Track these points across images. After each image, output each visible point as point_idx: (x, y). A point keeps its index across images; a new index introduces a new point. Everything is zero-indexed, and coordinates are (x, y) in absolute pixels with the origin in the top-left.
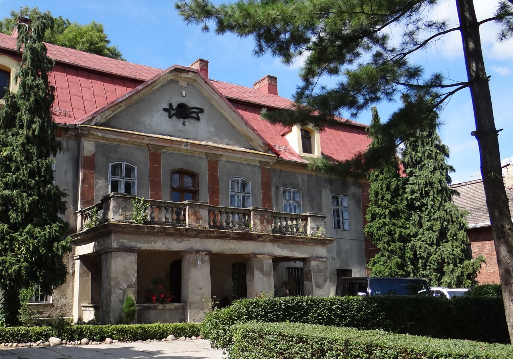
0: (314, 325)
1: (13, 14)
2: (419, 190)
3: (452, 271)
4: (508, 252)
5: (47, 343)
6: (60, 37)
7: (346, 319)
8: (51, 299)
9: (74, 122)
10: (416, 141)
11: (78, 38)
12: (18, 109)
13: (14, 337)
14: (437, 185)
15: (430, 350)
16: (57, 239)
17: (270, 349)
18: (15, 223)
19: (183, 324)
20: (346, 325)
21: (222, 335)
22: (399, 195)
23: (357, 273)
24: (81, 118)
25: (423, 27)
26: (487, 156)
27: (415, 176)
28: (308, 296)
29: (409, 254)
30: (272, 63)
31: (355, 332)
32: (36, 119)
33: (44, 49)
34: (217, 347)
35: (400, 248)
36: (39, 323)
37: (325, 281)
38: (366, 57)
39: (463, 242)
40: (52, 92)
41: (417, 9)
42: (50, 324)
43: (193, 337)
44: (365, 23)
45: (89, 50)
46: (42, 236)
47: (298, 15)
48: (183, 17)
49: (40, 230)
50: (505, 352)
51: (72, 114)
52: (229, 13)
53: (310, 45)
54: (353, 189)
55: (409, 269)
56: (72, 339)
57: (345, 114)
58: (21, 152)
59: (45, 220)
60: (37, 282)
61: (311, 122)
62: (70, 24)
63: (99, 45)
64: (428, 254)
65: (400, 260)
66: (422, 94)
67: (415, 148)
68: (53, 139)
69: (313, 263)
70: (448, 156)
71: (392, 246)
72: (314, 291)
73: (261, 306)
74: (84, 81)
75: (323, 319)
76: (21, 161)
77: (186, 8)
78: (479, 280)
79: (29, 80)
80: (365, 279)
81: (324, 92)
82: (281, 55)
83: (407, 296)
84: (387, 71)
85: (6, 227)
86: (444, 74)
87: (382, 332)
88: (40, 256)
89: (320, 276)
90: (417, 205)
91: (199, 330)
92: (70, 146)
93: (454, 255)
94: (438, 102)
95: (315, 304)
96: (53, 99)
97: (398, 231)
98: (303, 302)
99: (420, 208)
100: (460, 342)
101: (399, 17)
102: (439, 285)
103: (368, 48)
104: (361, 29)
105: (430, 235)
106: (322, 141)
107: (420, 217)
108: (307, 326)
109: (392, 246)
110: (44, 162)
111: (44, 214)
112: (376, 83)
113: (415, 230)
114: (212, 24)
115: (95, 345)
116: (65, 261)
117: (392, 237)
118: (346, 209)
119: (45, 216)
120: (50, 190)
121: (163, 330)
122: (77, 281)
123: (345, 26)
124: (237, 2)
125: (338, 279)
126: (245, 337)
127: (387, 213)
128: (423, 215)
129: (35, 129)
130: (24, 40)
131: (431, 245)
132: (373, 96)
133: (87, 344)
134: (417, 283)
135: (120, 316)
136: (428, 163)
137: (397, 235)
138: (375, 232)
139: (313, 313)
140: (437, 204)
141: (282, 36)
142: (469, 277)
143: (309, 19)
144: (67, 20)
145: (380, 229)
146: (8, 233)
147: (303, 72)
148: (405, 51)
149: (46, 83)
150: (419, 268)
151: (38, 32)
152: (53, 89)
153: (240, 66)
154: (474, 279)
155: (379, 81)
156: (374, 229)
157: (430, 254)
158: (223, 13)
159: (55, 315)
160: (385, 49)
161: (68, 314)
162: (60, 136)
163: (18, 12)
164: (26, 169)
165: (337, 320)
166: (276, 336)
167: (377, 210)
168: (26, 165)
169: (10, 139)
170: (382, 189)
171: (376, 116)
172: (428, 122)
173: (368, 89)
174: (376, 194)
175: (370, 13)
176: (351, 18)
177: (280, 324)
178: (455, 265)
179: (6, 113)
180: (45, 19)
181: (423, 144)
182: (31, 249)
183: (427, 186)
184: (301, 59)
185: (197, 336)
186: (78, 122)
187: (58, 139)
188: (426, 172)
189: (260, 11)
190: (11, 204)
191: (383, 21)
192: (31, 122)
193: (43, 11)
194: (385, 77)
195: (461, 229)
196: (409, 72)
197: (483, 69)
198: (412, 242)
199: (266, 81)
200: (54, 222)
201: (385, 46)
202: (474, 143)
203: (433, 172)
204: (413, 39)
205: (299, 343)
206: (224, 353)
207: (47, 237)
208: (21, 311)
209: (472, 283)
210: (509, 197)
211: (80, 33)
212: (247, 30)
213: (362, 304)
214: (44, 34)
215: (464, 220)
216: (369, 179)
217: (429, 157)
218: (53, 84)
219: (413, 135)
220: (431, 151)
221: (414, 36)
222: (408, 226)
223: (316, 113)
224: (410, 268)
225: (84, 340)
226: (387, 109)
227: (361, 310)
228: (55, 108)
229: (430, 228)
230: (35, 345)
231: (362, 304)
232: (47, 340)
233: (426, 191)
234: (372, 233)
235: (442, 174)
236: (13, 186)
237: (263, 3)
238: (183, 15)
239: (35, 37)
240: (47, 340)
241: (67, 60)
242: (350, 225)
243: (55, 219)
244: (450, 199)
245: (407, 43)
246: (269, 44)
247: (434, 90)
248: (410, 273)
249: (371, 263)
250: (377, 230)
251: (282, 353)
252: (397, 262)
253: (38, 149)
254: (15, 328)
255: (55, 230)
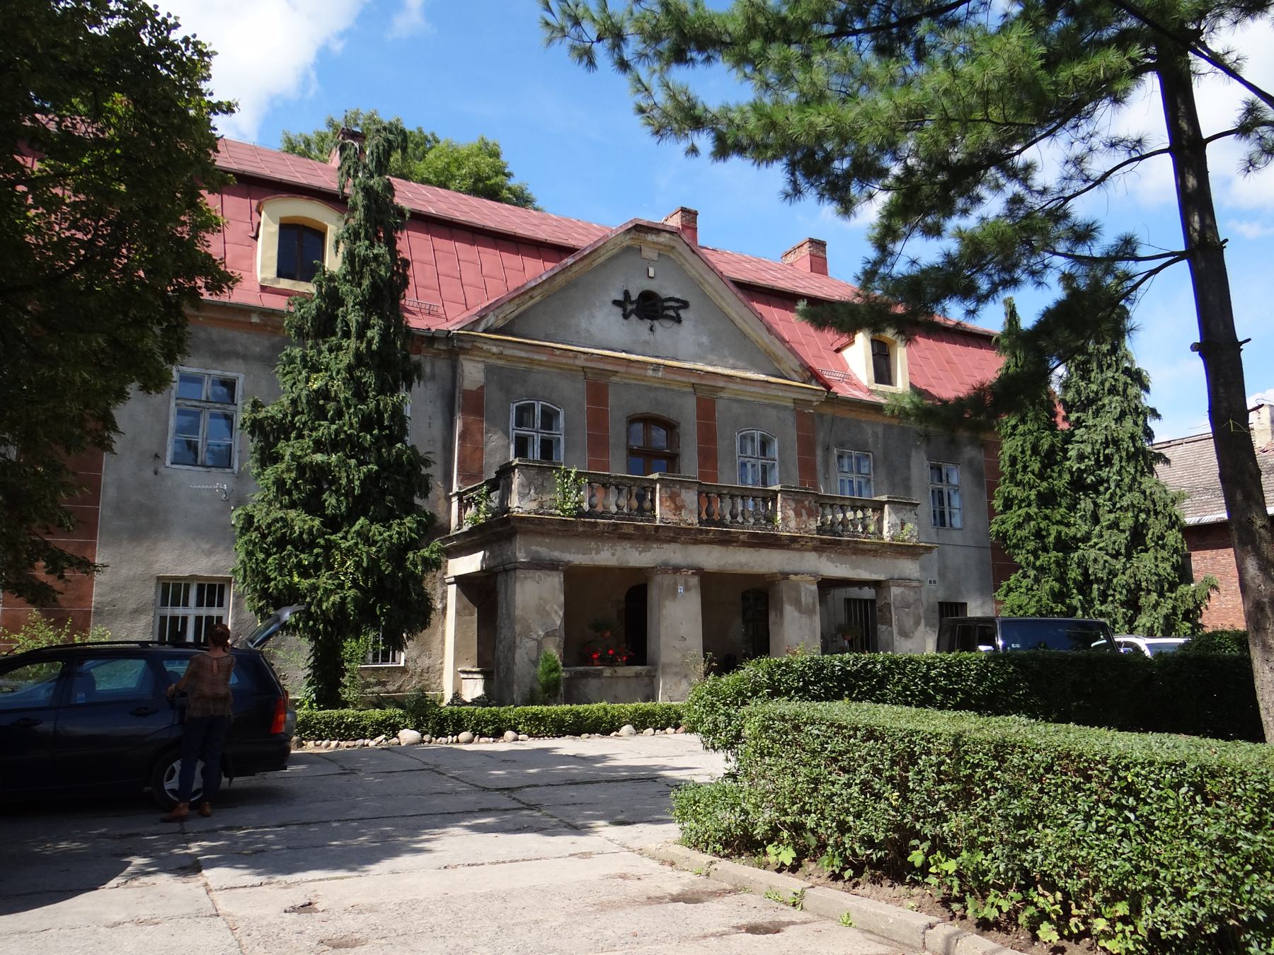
0: (895, 707)
1: (331, 123)
2: (1093, 453)
3: (1156, 606)
4: (1260, 569)
5: (395, 740)
6: (420, 167)
7: (955, 696)
8: (402, 658)
9: (445, 326)
10: (1088, 362)
11: (453, 169)
12: (341, 303)
13: (333, 729)
14: (1127, 444)
15: (1114, 754)
16: (413, 545)
17: (814, 752)
18: (335, 516)
19: (649, 705)
20: (957, 707)
21: (722, 725)
22: (1056, 463)
23: (976, 609)
24: (458, 319)
25: (1101, 147)
26: (1221, 390)
27: (1086, 427)
28: (885, 652)
29: (1074, 573)
30: (817, 215)
31: (973, 719)
32: (374, 320)
33: (390, 188)
34: (713, 747)
35: (1057, 563)
36: (379, 704)
37: (917, 624)
38: (993, 204)
39: (1176, 551)
40: (405, 270)
41: (1089, 115)
42: (401, 706)
43: (669, 730)
44: (992, 140)
45: (475, 191)
46: (384, 540)
47: (866, 125)
48: (649, 129)
49: (382, 529)
50: (1254, 758)
51: (441, 311)
52: (737, 121)
53: (889, 181)
54: (969, 452)
55: (1075, 602)
56: (441, 733)
57: (954, 311)
58: (346, 382)
59: (392, 509)
60: (375, 625)
61: (890, 326)
62: (438, 142)
63: (493, 181)
64: (1110, 573)
65: (1057, 585)
66: (1099, 273)
67: (1086, 376)
68: (406, 357)
69: (895, 591)
70: (1147, 389)
71: (1043, 559)
72: (896, 643)
73: (796, 670)
74: (464, 250)
75: (913, 695)
76: (346, 399)
77: (656, 113)
78: (1206, 623)
79: (362, 248)
80: (991, 620)
81: (914, 270)
82: (834, 199)
83: (1071, 652)
84: (1034, 231)
85: (317, 522)
86: (1141, 235)
87: (1024, 719)
88: (382, 577)
89: (908, 614)
90: (1089, 481)
91: (680, 717)
92: (437, 371)
93: (1159, 575)
94: (1128, 289)
95: (898, 667)
96: (405, 283)
97: (1054, 530)
98: (874, 664)
99: (1094, 487)
100: (1170, 739)
101: (1055, 129)
102: (1131, 632)
103: (998, 187)
104: (984, 151)
105: (1113, 538)
106: (912, 362)
107: (1095, 504)
108: (884, 708)
109: (1043, 559)
110: (389, 401)
111: (389, 498)
112: (1013, 253)
113: (1085, 528)
114: (705, 141)
115: (486, 745)
116: (428, 587)
117: (1043, 542)
118: (957, 489)
119: (390, 501)
120: (400, 454)
121: (613, 716)
122: (451, 624)
123: (954, 146)
124: (751, 100)
125: (941, 621)
126: (766, 729)
127: (1033, 497)
128: (1100, 501)
129: (373, 338)
130: (352, 171)
131: (1116, 556)
132: (1007, 277)
133: (470, 741)
134: (1090, 629)
135: (532, 690)
136: (1111, 402)
137: (1051, 539)
138: (1011, 532)
139: (894, 685)
140: (1127, 480)
141: (836, 164)
142: (1187, 616)
143: (887, 133)
144: (433, 135)
145: (1019, 526)
146: (322, 535)
147: (875, 233)
148: (1067, 193)
149: (393, 252)
150: (1092, 600)
151: (378, 158)
152: (406, 263)
153: (758, 221)
154: (1196, 620)
155: (1019, 249)
156: (1009, 527)
157: (1113, 573)
158: (725, 121)
159: (410, 687)
160: (1029, 188)
161: (433, 686)
162: (419, 352)
163: (340, 120)
164: (355, 414)
165: (938, 698)
166: (824, 728)
167: (1015, 491)
168: (356, 406)
169: (326, 357)
170: (1023, 452)
171: (1012, 315)
172: (1109, 325)
173: (997, 263)
174: (1013, 461)
175: (1001, 121)
176: (965, 130)
177: (832, 704)
178: (1161, 595)
179: (319, 308)
180: (391, 132)
181: (1100, 367)
182: (365, 564)
183: (1107, 447)
184: (872, 208)
185: (677, 727)
186: (453, 327)
187: (415, 358)
188: (1107, 421)
189: (794, 117)
190: (327, 479)
191: (1026, 137)
192: (364, 326)
193: (386, 118)
194: (1029, 242)
195: (1172, 525)
196: (1075, 232)
197: (1213, 227)
198: (1080, 552)
199: (806, 250)
200: (408, 514)
201: (1030, 183)
202: (1197, 365)
203: (1120, 419)
204: (1082, 171)
205: (868, 740)
206: (728, 760)
207: (394, 541)
208: (344, 680)
209: (1192, 629)
210: (1263, 467)
211: (456, 160)
212: (770, 154)
213: (986, 666)
214: (388, 160)
215: (1177, 509)
216: (998, 432)
217: (1113, 391)
218: (406, 255)
219: (1082, 350)
220: (1116, 380)
221: (1084, 165)
222: (1072, 520)
223: (900, 310)
224: (1076, 600)
225: (464, 736)
226: (1033, 301)
227: (985, 678)
228: (409, 299)
229: (1114, 525)
230: (372, 743)
231: (986, 666)
232: (395, 735)
233: (1106, 456)
234: (1005, 534)
235: (1136, 423)
236: (333, 445)
237: (799, 103)
238: (649, 124)
239: (372, 167)
240: (395, 735)
241: (432, 210)
242: (963, 520)
243: (410, 509)
244: (1152, 471)
245: (1071, 178)
246: (812, 180)
247: (1122, 266)
248: (1076, 609)
249: (1002, 591)
250: (1015, 529)
251: (835, 760)
252: (1052, 589)
253: (377, 377)
254: (335, 713)
255: (410, 529)
